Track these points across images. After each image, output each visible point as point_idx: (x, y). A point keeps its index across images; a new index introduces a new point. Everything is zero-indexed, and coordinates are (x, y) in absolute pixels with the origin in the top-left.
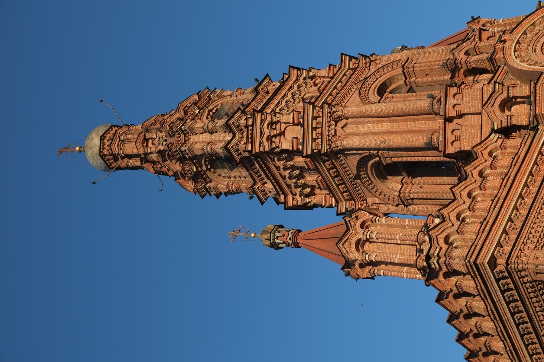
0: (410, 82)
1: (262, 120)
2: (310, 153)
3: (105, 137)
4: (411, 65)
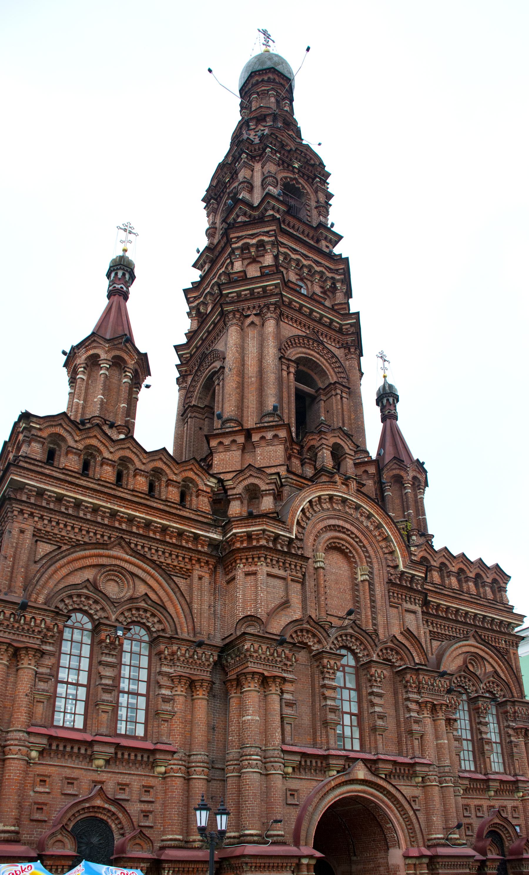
2: (224, 292)
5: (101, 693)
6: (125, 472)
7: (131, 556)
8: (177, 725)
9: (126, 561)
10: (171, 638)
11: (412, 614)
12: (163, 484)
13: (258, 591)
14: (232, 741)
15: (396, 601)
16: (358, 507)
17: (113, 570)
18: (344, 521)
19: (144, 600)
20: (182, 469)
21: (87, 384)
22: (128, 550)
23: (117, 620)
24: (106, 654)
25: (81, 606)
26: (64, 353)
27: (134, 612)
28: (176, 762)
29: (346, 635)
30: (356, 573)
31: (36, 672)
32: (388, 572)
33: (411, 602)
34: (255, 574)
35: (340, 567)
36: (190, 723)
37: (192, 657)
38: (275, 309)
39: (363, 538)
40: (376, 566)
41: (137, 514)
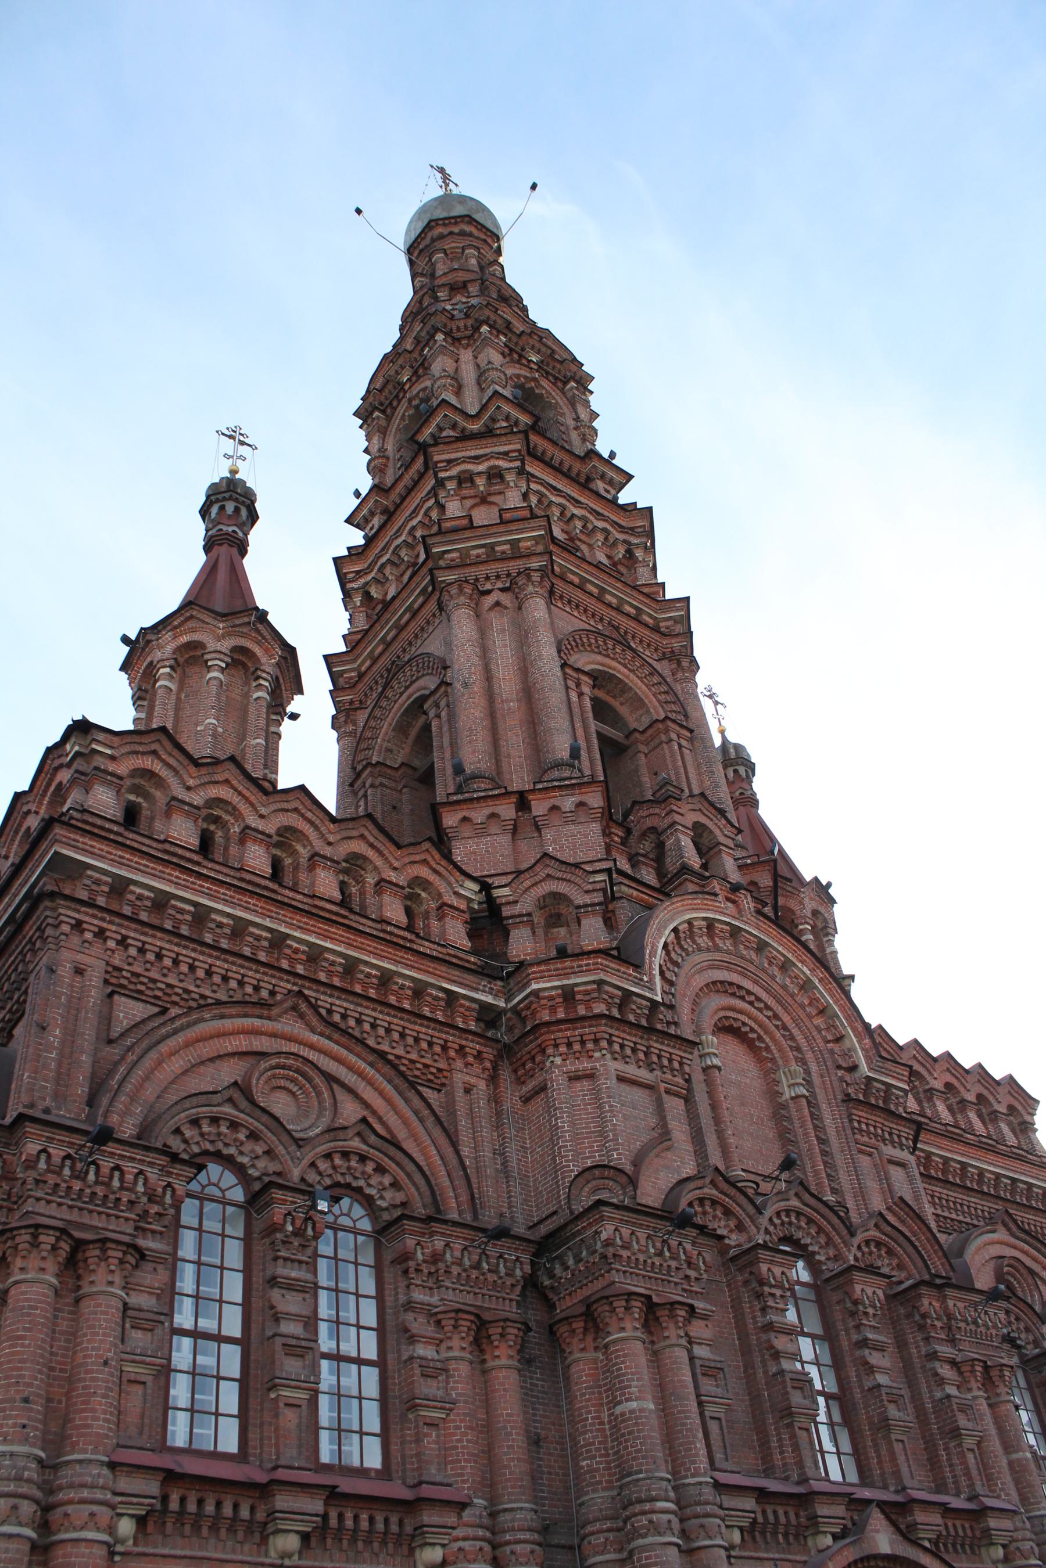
0: (636, 741)
1: (506, 453)
2: (435, 550)
3: (469, 223)
4: (674, 736)
5: (273, 1361)
6: (288, 861)
7: (321, 1034)
8: (462, 1436)
9: (312, 1047)
10: (430, 1219)
11: (899, 1169)
12: (370, 889)
13: (601, 1111)
14: (592, 1471)
15: (866, 1139)
16: (762, 947)
17: (283, 1067)
18: (740, 973)
19: (359, 1134)
20: (407, 860)
21: (178, 699)
22: (315, 1021)
23: (303, 1180)
24: (285, 1259)
25: (220, 1145)
26: (125, 640)
27: (338, 1161)
28: (470, 1532)
29: (788, 1212)
30: (778, 1082)
31: (125, 1304)
33: (892, 1142)
34: (591, 1076)
35: (743, 1070)
36: (487, 1428)
37: (477, 1266)
38: (542, 577)
40: (814, 1068)
41: (328, 945)
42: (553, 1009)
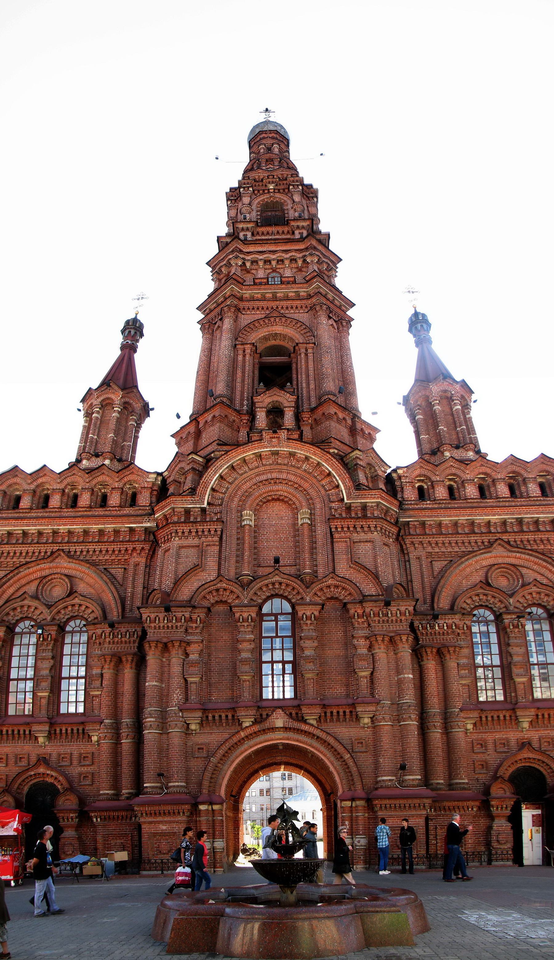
16: (292, 455)
29: (273, 584)
32: (331, 508)
39: (302, 482)
42: (110, 537)
